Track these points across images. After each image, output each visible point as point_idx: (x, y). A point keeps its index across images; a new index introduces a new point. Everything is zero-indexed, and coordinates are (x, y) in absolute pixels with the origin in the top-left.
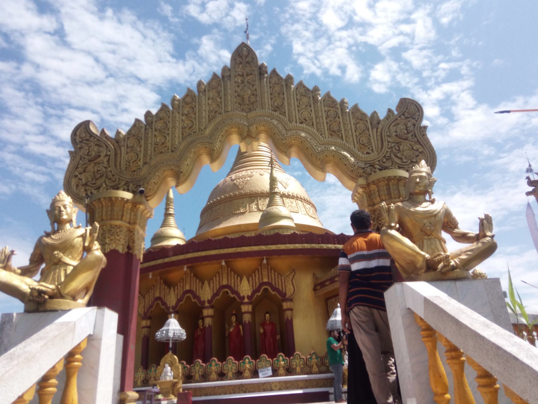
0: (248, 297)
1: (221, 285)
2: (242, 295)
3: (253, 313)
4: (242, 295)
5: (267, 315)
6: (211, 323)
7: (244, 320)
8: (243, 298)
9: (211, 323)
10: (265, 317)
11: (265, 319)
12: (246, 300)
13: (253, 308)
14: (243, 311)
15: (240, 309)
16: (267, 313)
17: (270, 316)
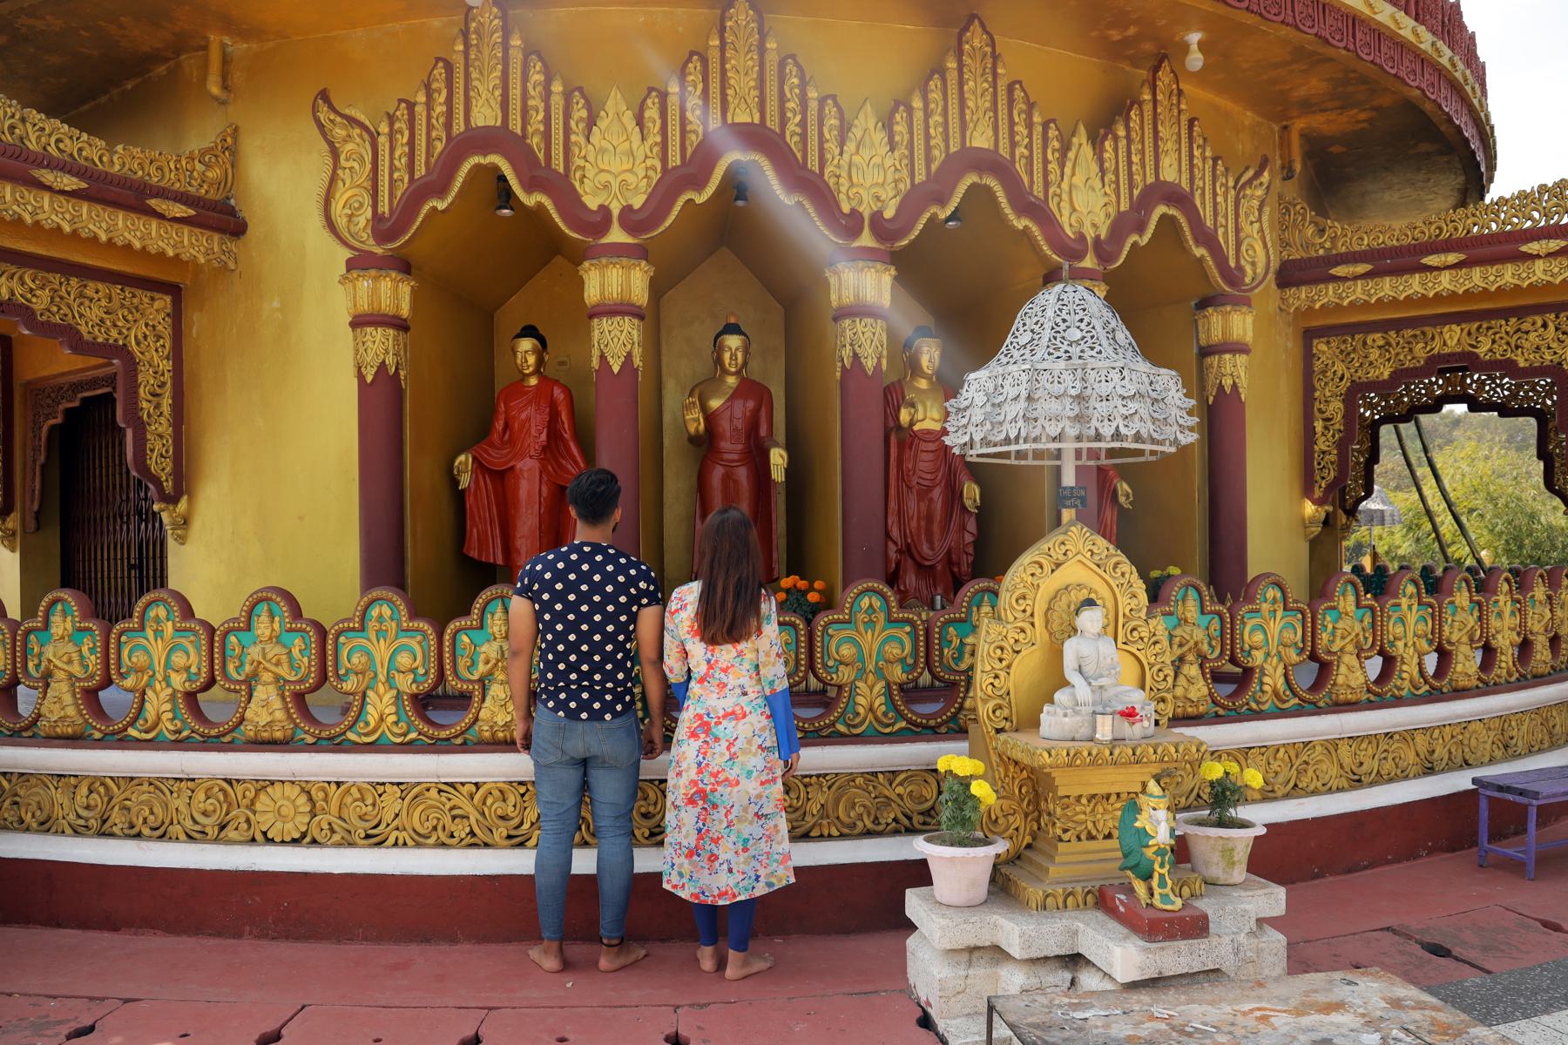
0: (629, 219)
1: (459, 127)
2: (592, 203)
3: (651, 317)
4: (592, 203)
5: (733, 341)
6: (390, 360)
7: (596, 353)
8: (602, 220)
9: (390, 360)
10: (718, 348)
11: (719, 361)
12: (617, 235)
13: (657, 289)
14: (593, 292)
15: (580, 284)
16: (732, 329)
17: (746, 349)
